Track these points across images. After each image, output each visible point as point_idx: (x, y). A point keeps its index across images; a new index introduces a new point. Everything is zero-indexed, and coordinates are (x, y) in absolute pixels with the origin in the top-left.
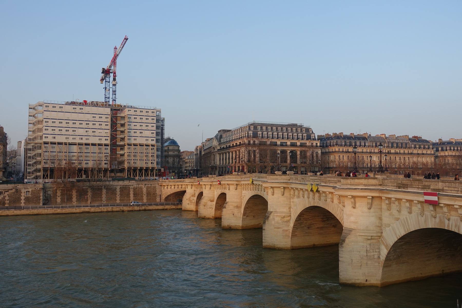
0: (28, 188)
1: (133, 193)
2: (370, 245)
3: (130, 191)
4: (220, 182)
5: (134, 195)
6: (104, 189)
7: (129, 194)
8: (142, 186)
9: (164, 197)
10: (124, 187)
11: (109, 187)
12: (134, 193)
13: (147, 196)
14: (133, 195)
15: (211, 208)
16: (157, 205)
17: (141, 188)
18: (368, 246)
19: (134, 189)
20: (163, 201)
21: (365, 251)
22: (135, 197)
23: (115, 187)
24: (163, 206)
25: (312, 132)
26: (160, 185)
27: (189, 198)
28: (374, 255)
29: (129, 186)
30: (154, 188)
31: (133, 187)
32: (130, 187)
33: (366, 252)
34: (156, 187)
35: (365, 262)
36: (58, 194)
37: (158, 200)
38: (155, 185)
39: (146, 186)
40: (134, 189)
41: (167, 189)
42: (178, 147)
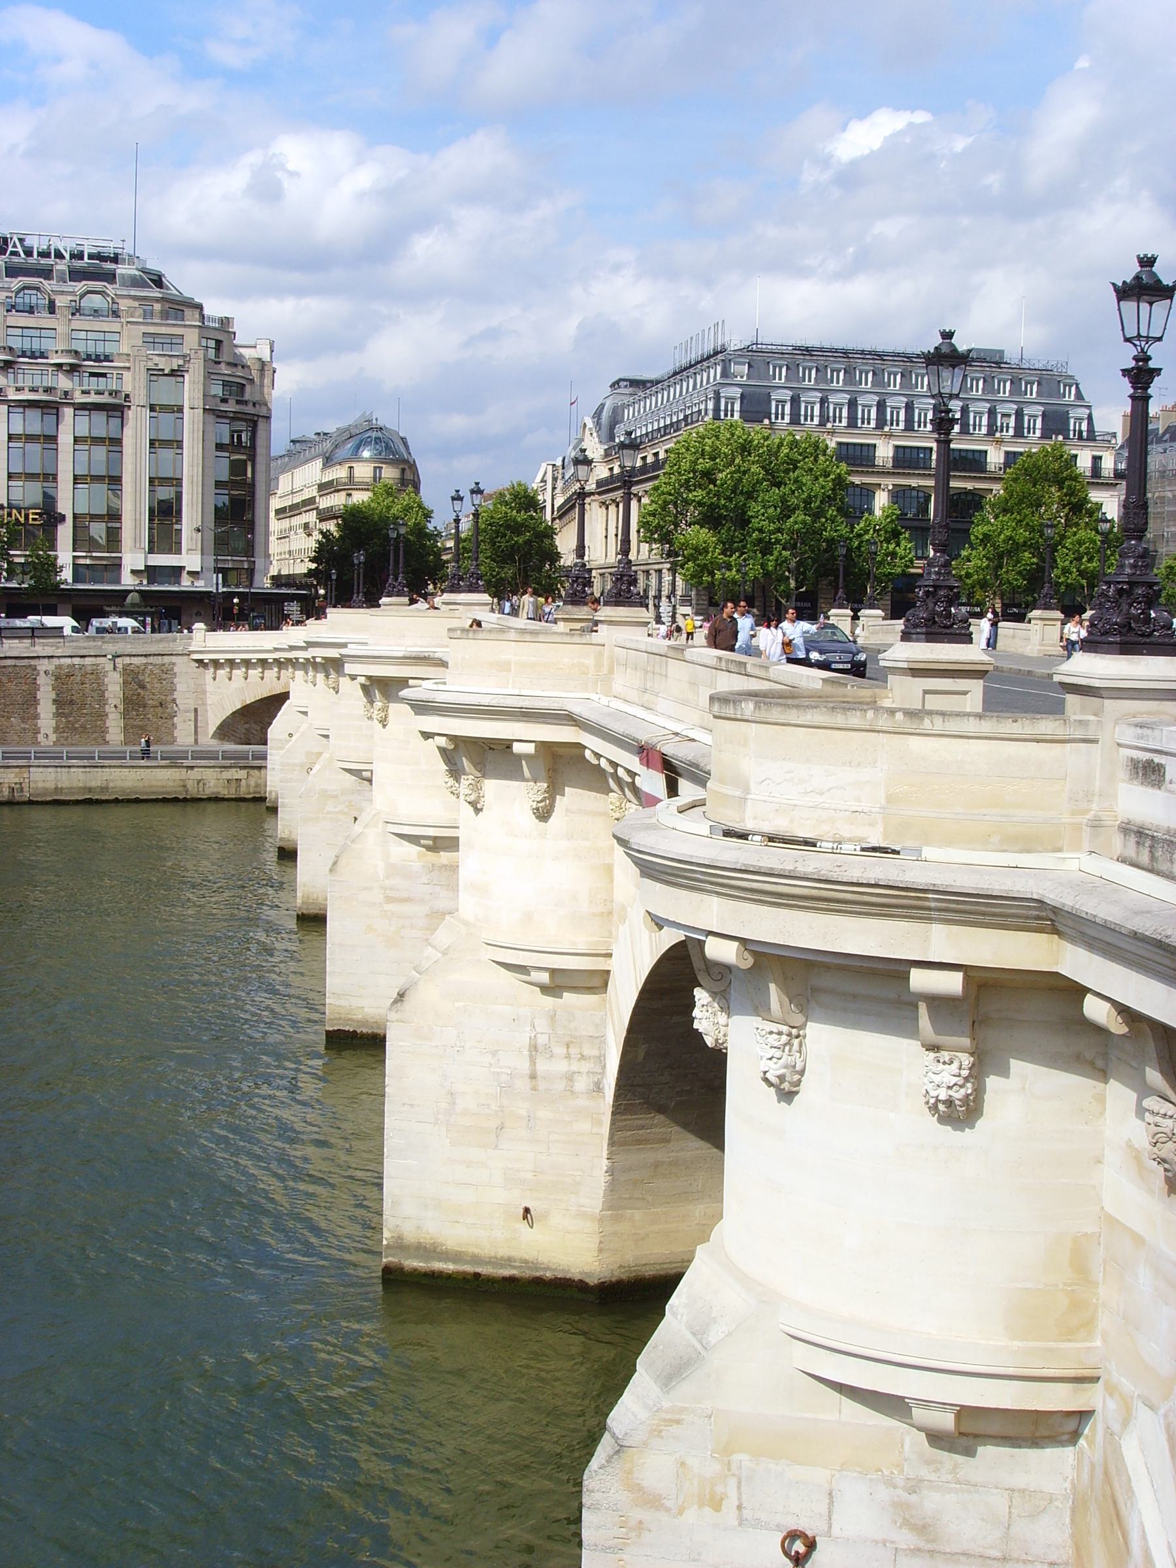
2: (552, 1017)
3: (35, 686)
5: (57, 709)
7: (32, 700)
9: (214, 719)
12: (58, 695)
13: (125, 715)
14: (53, 708)
16: (174, 760)
17: (97, 675)
18: (542, 1025)
20: (208, 740)
21: (526, 1053)
25: (1079, 396)
26: (197, 661)
28: (570, 1077)
29: (33, 662)
30: (165, 676)
31: (51, 668)
32: (38, 668)
33: (531, 1056)
35: (524, 1113)
37: (183, 736)
38: (166, 659)
39: (118, 660)
40: (62, 679)
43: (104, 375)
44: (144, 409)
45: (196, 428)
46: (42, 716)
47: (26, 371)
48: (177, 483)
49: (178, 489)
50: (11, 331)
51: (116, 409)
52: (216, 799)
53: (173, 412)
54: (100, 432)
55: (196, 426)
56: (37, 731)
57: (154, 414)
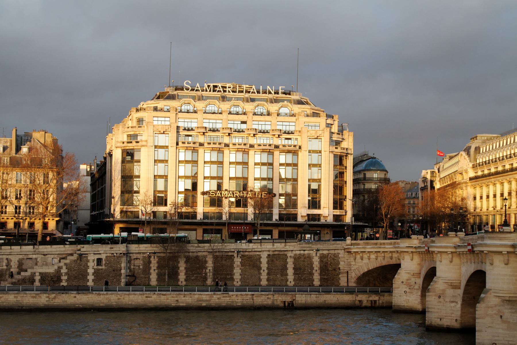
0: (100, 252)
1: (293, 266)
4: (472, 248)
5: (295, 272)
6: (237, 257)
8: (311, 252)
9: (354, 276)
10: (275, 255)
11: (247, 253)
12: (295, 266)
13: (321, 274)
14: (293, 271)
15: (453, 302)
16: (340, 291)
17: (310, 257)
19: (297, 259)
20: (352, 284)
22: (297, 276)
23: (258, 253)
24: (354, 296)
27: (407, 280)
29: (285, 253)
30: (335, 258)
31: (293, 255)
32: (288, 255)
34: (340, 256)
36: (152, 265)
37: (343, 281)
38: (336, 252)
39: (318, 252)
41: (361, 260)
42: (385, 173)
43: (290, 139)
44: (306, 152)
45: (326, 159)
46: (289, 275)
47: (261, 138)
48: (319, 181)
49: (320, 183)
50: (254, 122)
51: (294, 152)
52: (366, 308)
53: (318, 153)
54: (290, 161)
55: (326, 158)
56: (287, 280)
57: (310, 154)
